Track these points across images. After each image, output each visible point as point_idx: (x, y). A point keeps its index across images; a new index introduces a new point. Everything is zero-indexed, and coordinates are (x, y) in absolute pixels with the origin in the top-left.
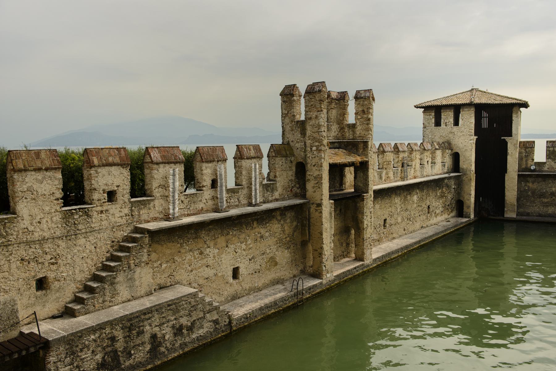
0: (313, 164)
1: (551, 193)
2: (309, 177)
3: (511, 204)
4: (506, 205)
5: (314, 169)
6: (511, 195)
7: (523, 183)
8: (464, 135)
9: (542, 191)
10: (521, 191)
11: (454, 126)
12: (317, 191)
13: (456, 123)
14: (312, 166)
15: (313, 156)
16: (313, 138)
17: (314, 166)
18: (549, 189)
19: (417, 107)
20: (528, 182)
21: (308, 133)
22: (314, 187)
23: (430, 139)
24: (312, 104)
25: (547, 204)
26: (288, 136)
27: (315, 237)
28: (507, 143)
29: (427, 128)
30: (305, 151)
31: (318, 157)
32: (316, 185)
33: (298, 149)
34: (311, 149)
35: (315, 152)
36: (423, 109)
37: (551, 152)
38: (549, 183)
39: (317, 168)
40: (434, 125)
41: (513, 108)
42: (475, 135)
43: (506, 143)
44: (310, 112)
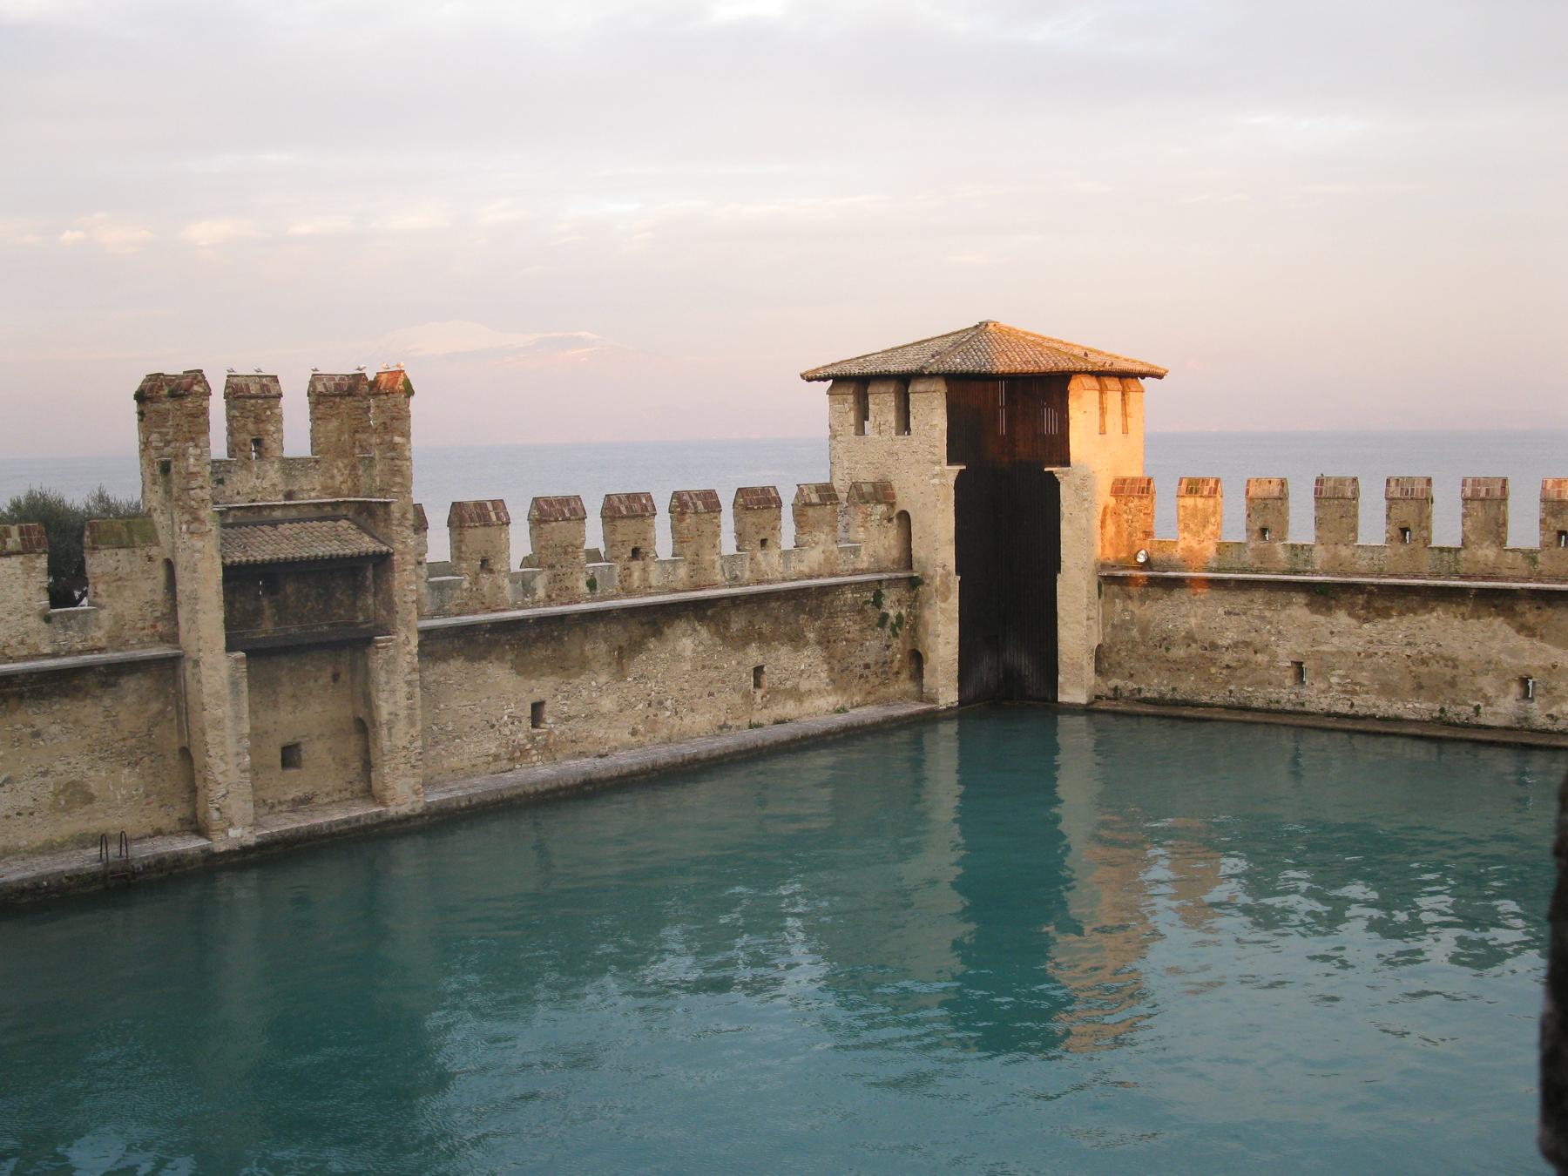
1: (1187, 633)
3: (1073, 664)
4: (1061, 667)
6: (1073, 637)
7: (1117, 601)
8: (917, 461)
9: (1164, 627)
10: (1114, 626)
11: (897, 434)
13: (904, 425)
18: (1182, 620)
19: (810, 378)
23: (846, 472)
29: (838, 438)
36: (831, 381)
37: (1188, 511)
38: (1183, 603)
40: (853, 429)
42: (948, 465)
43: (1057, 484)
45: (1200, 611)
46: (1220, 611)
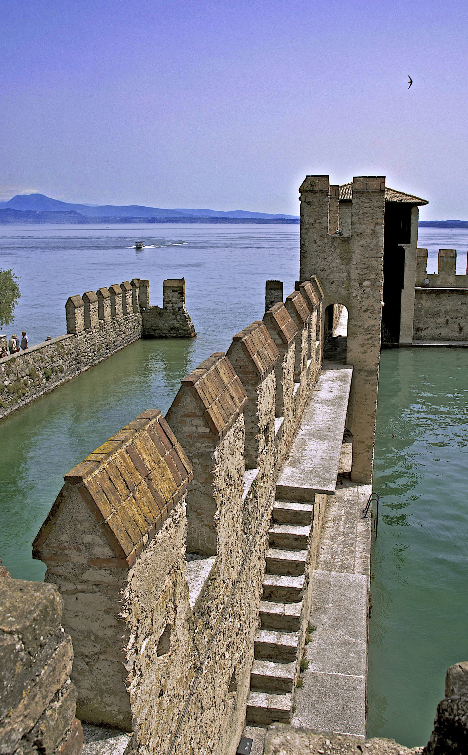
0: (364, 308)
2: (354, 328)
5: (365, 315)
6: (408, 316)
9: (435, 310)
12: (369, 351)
14: (361, 310)
15: (364, 296)
16: (365, 266)
17: (365, 311)
18: (443, 307)
20: (421, 298)
21: (356, 257)
22: (363, 345)
24: (365, 211)
25: (441, 325)
26: (314, 260)
27: (360, 423)
28: (405, 251)
30: (348, 287)
31: (374, 297)
32: (367, 342)
33: (333, 282)
34: (360, 284)
35: (368, 290)
39: (370, 315)
41: (411, 208)
43: (403, 251)
44: (360, 224)
45: (451, 303)
46: (460, 303)
